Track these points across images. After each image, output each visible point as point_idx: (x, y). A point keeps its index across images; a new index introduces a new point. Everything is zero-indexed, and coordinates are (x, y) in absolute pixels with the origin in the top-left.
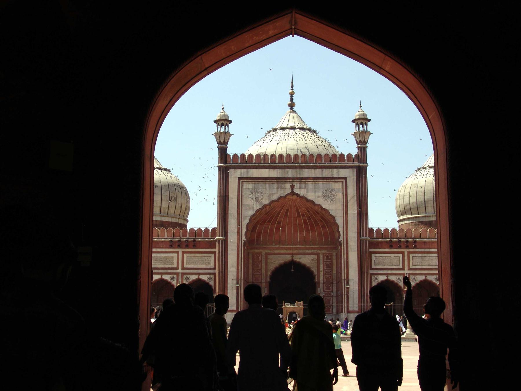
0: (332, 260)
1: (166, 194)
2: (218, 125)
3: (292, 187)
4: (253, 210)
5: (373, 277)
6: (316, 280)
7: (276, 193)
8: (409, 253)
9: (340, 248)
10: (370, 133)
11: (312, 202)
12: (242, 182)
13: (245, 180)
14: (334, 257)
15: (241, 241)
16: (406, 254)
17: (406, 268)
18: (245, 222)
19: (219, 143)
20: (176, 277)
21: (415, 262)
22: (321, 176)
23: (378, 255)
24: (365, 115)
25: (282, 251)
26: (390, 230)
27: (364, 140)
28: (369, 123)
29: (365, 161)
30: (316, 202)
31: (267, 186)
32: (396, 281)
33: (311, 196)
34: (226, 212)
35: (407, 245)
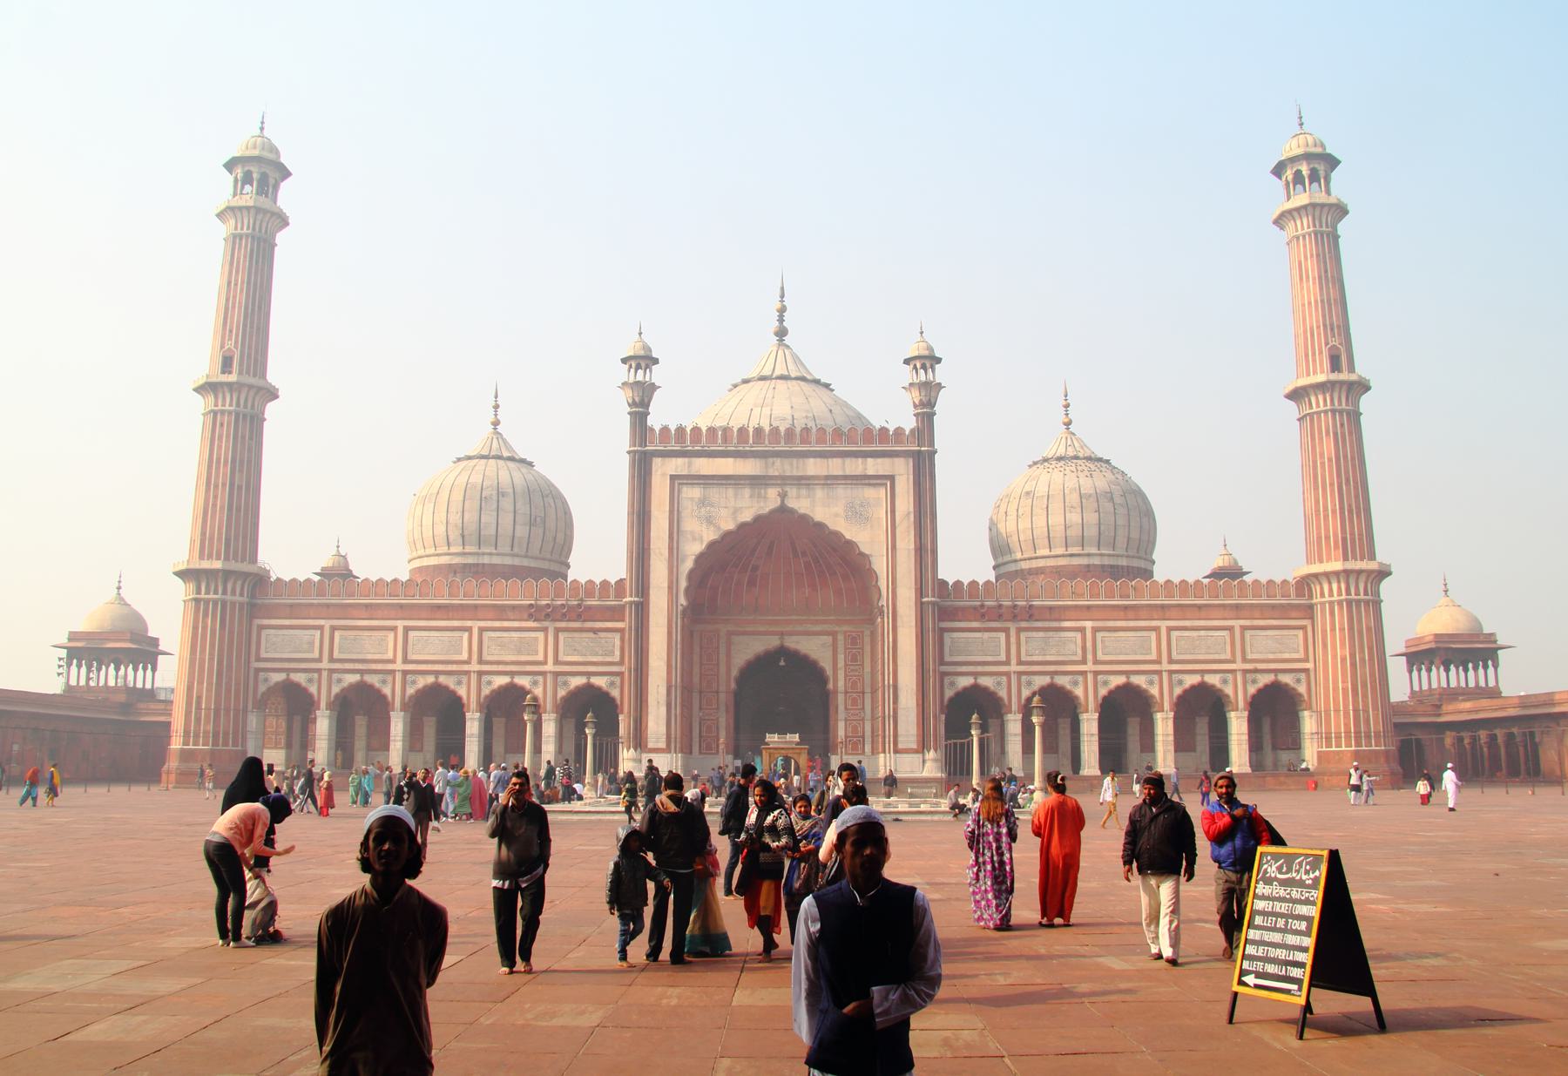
0: (863, 642)
1: (523, 508)
2: (631, 367)
3: (783, 496)
4: (702, 542)
5: (947, 680)
6: (830, 686)
7: (749, 507)
8: (1019, 630)
9: (879, 620)
10: (939, 386)
11: (820, 526)
12: (679, 484)
13: (685, 482)
14: (867, 640)
17: (1014, 661)
18: (688, 564)
19: (633, 404)
22: (841, 473)
23: (955, 635)
24: (930, 349)
25: (762, 629)
26: (981, 583)
27: (930, 400)
28: (937, 366)
29: (932, 443)
31: (731, 491)
32: (992, 688)
34: (646, 547)
35: (1015, 614)
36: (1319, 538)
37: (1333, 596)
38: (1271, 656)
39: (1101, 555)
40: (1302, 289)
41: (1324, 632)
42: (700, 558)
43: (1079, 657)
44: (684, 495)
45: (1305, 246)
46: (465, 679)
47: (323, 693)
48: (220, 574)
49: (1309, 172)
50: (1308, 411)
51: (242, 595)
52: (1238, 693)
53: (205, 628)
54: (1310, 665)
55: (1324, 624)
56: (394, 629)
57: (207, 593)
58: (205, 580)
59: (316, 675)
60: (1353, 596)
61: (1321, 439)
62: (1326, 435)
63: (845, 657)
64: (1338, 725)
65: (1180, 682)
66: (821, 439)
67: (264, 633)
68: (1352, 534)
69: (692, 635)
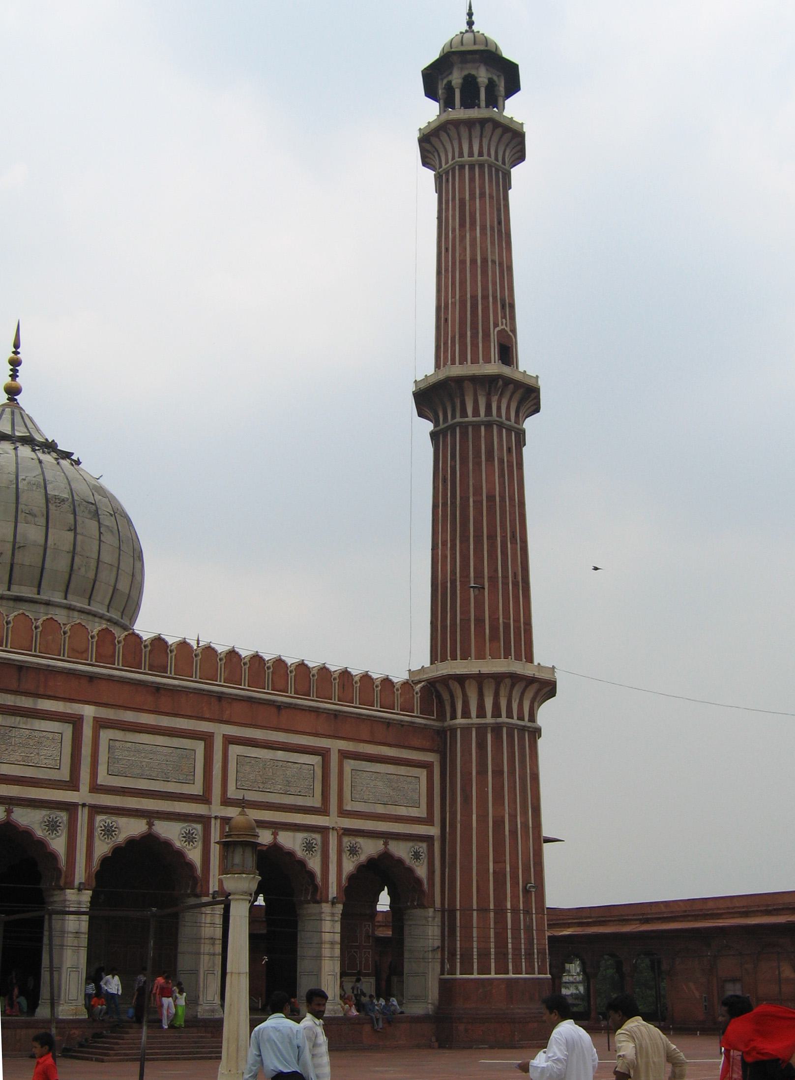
36: (466, 622)
37: (484, 716)
38: (380, 809)
39: (70, 608)
40: (463, 238)
43: (65, 774)
45: (472, 180)
49: (486, 81)
50: (458, 419)
54: (434, 831)
55: (467, 762)
60: (515, 721)
61: (477, 464)
62: (487, 460)
64: (484, 938)
68: (517, 621)
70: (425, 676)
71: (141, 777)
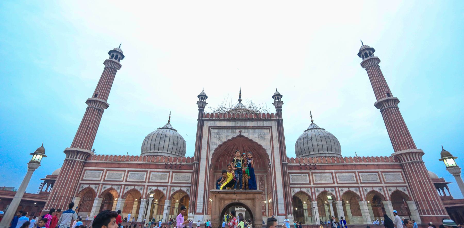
3: (240, 132)
4: (217, 145)
8: (312, 173)
9: (270, 169)
11: (251, 141)
12: (211, 128)
15: (208, 164)
16: (310, 174)
17: (312, 183)
18: (212, 152)
20: (166, 188)
21: (316, 179)
23: (293, 175)
30: (254, 141)
31: (225, 131)
33: (251, 137)
34: (201, 146)
37: (409, 161)
38: (393, 181)
41: (409, 173)
42: (216, 149)
43: (332, 182)
44: (212, 132)
46: (143, 187)
47: (99, 191)
48: (76, 152)
51: (82, 159)
52: (387, 194)
53: (66, 169)
54: (407, 184)
55: (408, 170)
56: (125, 171)
57: (71, 158)
58: (71, 154)
59: (98, 186)
63: (259, 183)
65: (366, 190)
66: (251, 117)
67: (86, 171)
69: (214, 176)
70: (394, 155)
71: (345, 181)
